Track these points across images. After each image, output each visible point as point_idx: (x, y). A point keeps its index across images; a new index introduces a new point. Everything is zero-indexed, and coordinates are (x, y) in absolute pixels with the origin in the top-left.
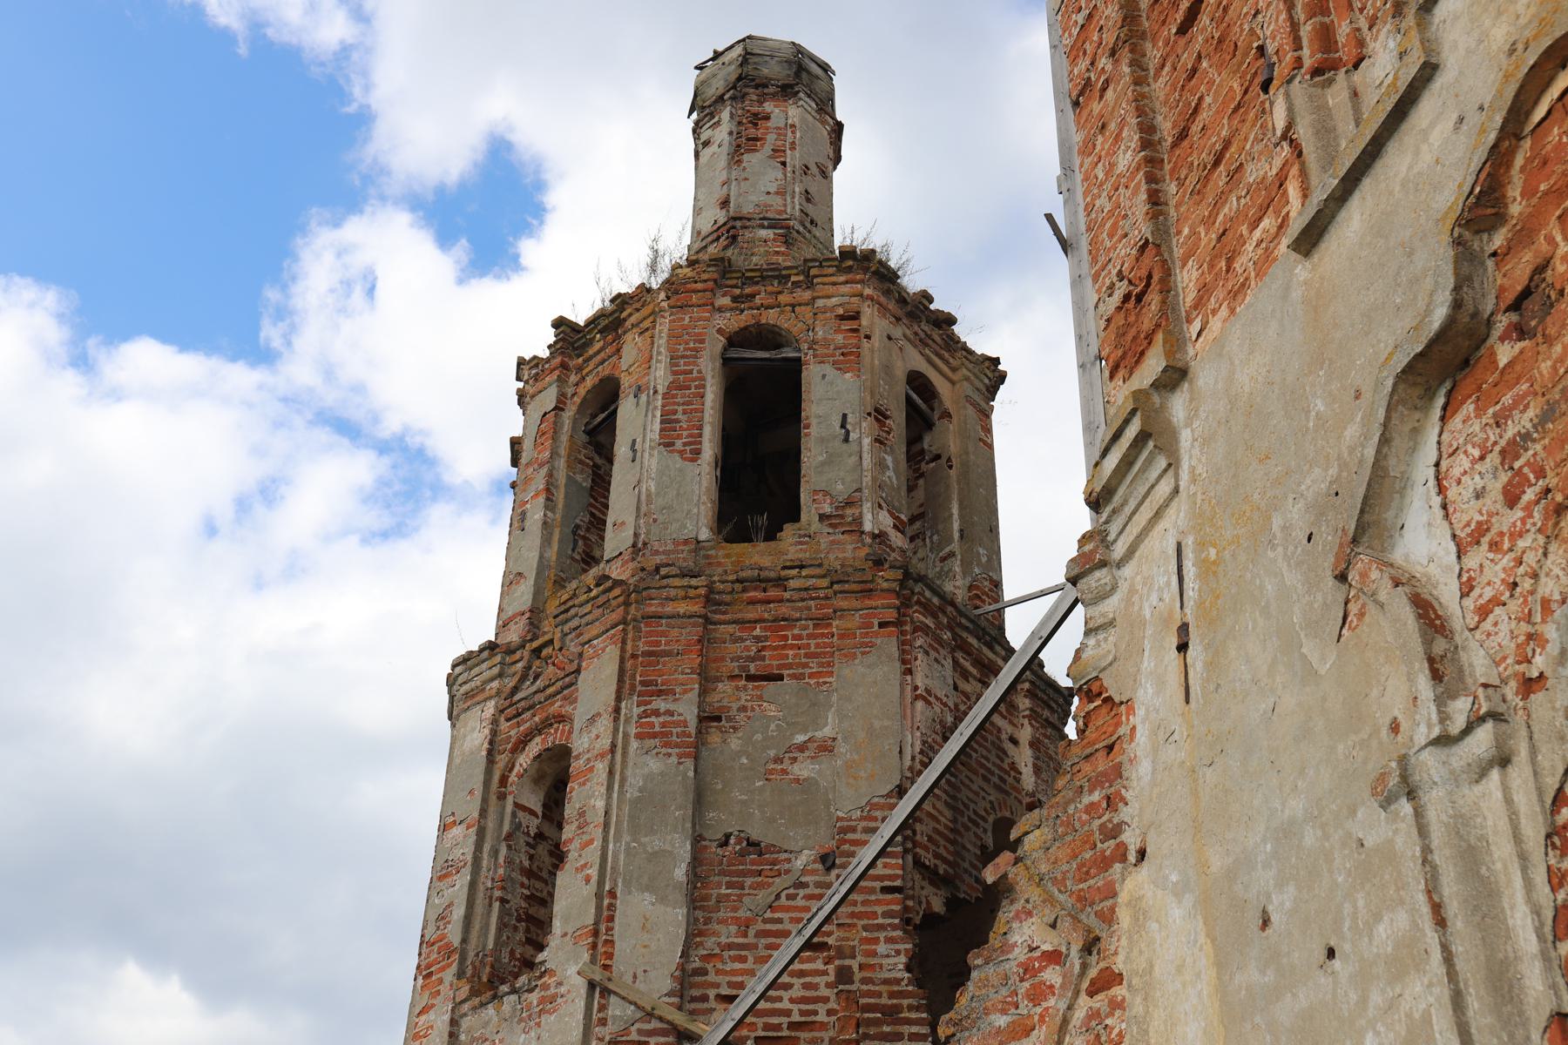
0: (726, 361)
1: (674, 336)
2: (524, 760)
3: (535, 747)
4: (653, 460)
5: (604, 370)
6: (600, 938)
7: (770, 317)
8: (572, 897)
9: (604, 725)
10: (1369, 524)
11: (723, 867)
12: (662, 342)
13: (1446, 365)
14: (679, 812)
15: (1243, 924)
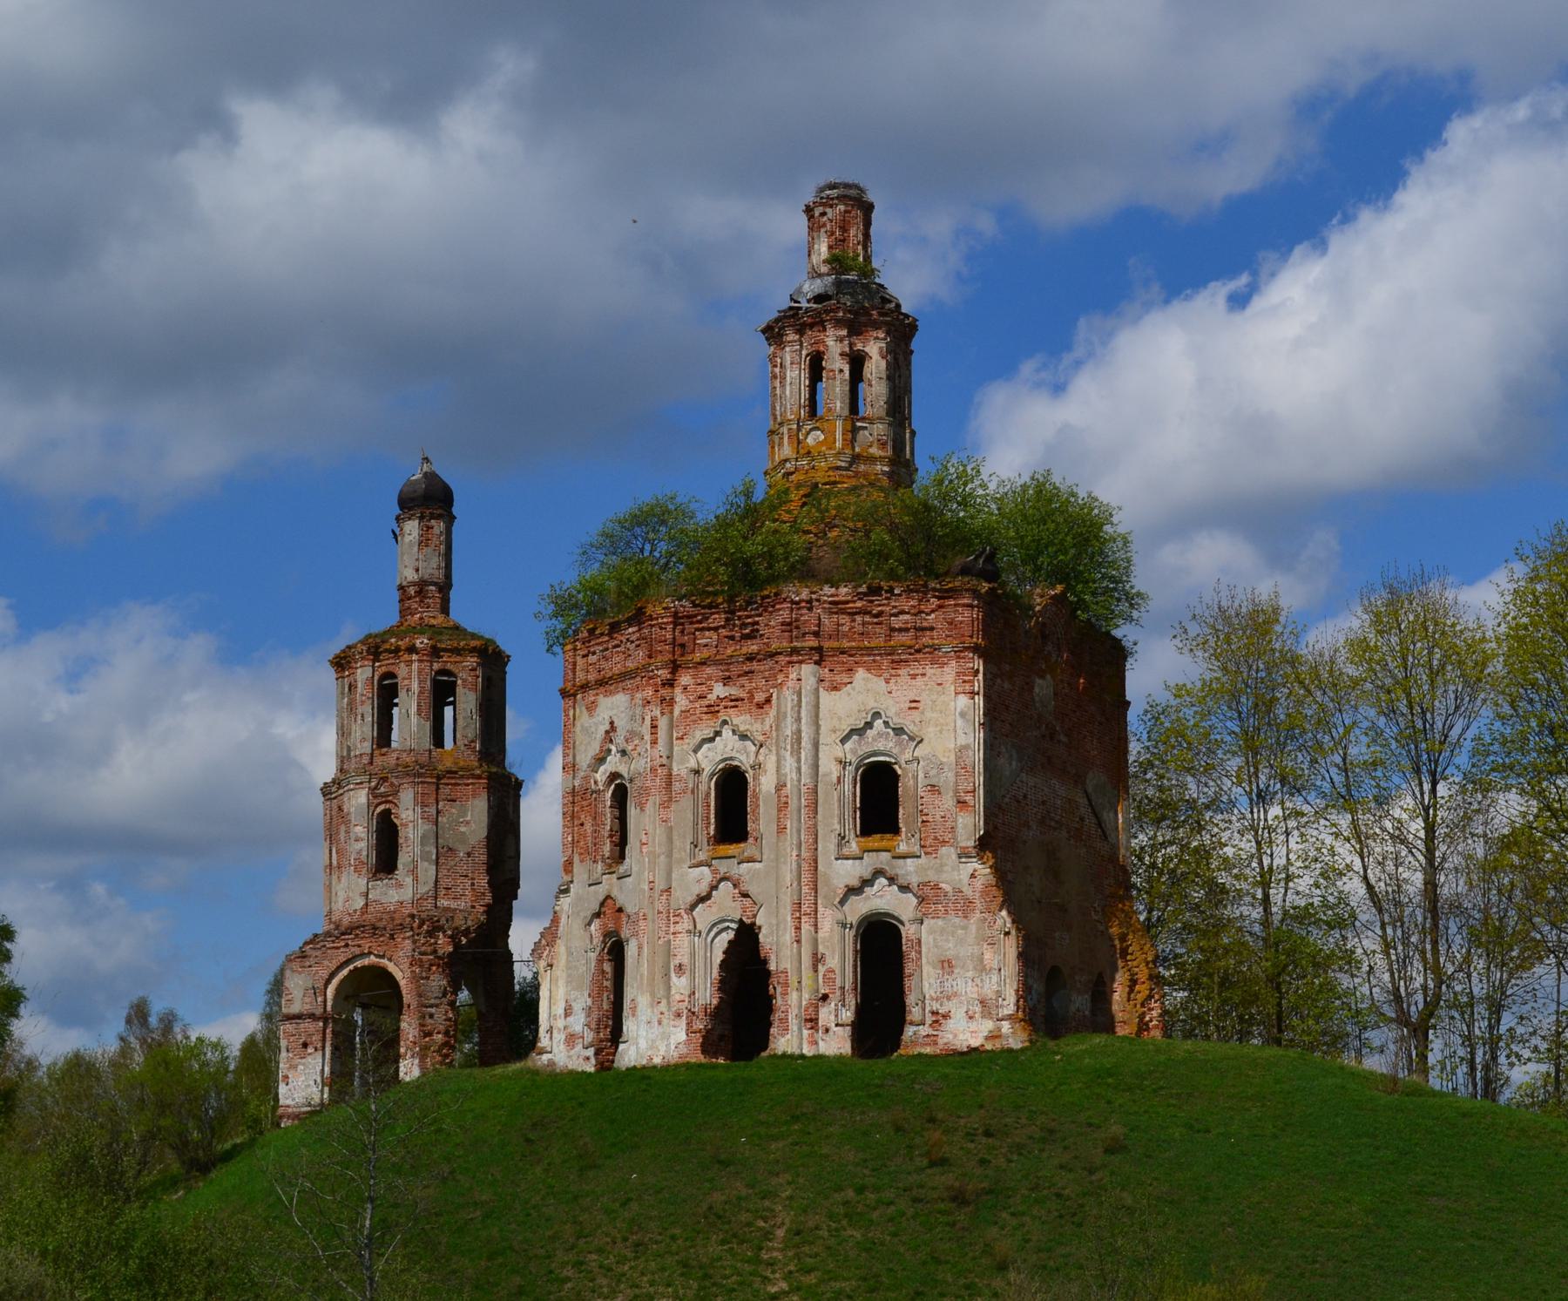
0: (435, 683)
1: (420, 672)
2: (379, 810)
3: (382, 807)
4: (414, 719)
5: (391, 668)
6: (413, 871)
7: (449, 666)
8: (403, 859)
9: (410, 812)
10: (589, 924)
11: (443, 853)
12: (415, 674)
13: (597, 915)
14: (433, 840)
15: (569, 953)
